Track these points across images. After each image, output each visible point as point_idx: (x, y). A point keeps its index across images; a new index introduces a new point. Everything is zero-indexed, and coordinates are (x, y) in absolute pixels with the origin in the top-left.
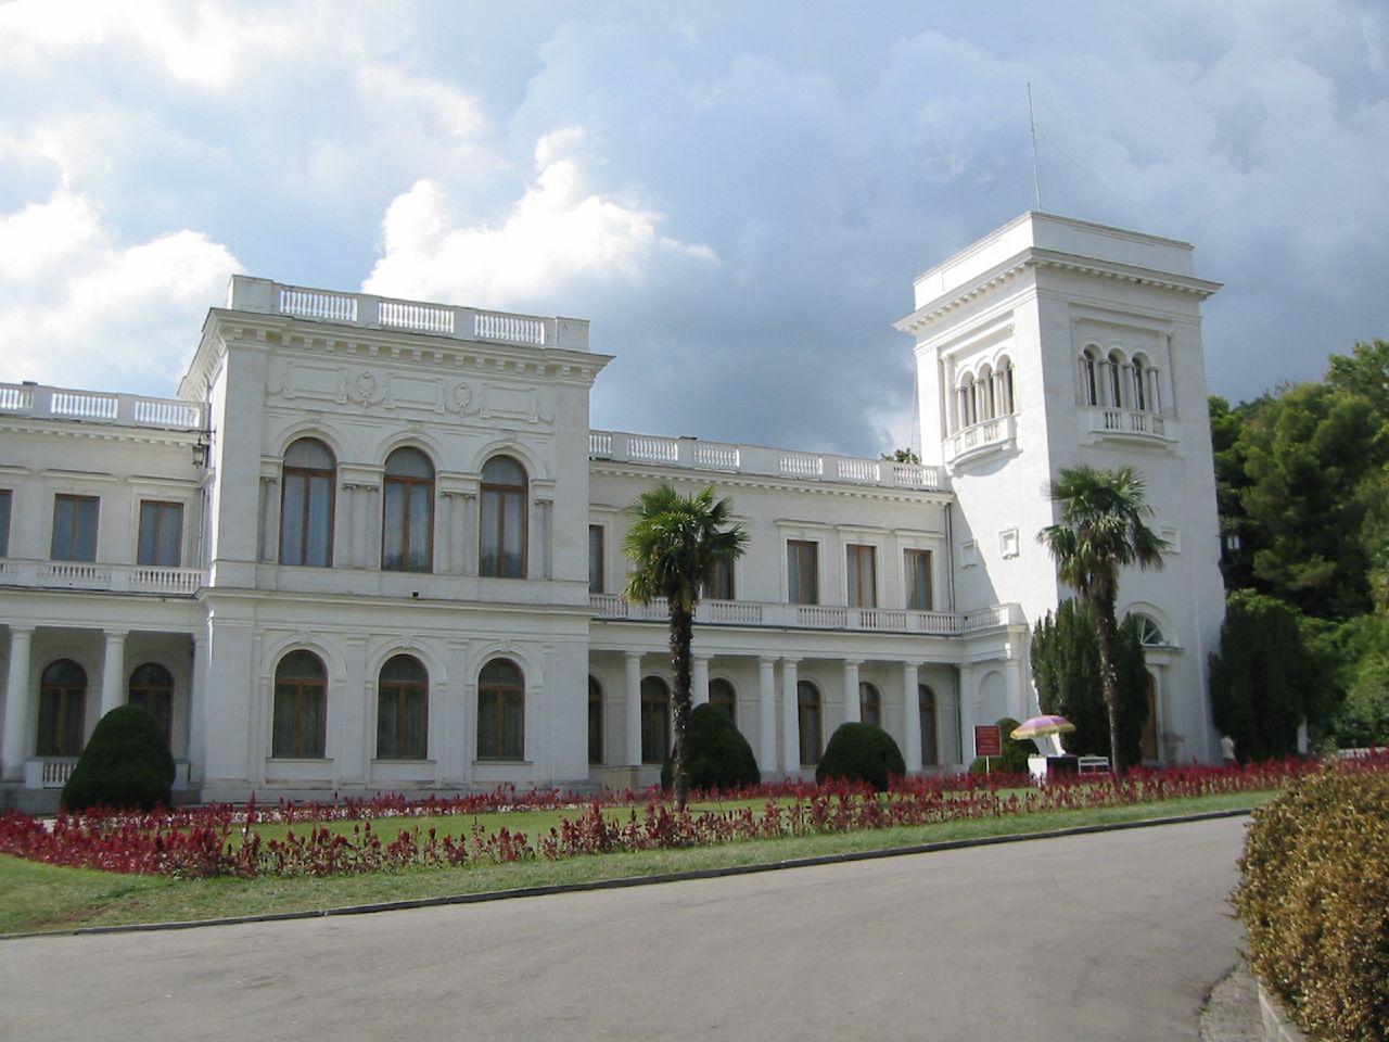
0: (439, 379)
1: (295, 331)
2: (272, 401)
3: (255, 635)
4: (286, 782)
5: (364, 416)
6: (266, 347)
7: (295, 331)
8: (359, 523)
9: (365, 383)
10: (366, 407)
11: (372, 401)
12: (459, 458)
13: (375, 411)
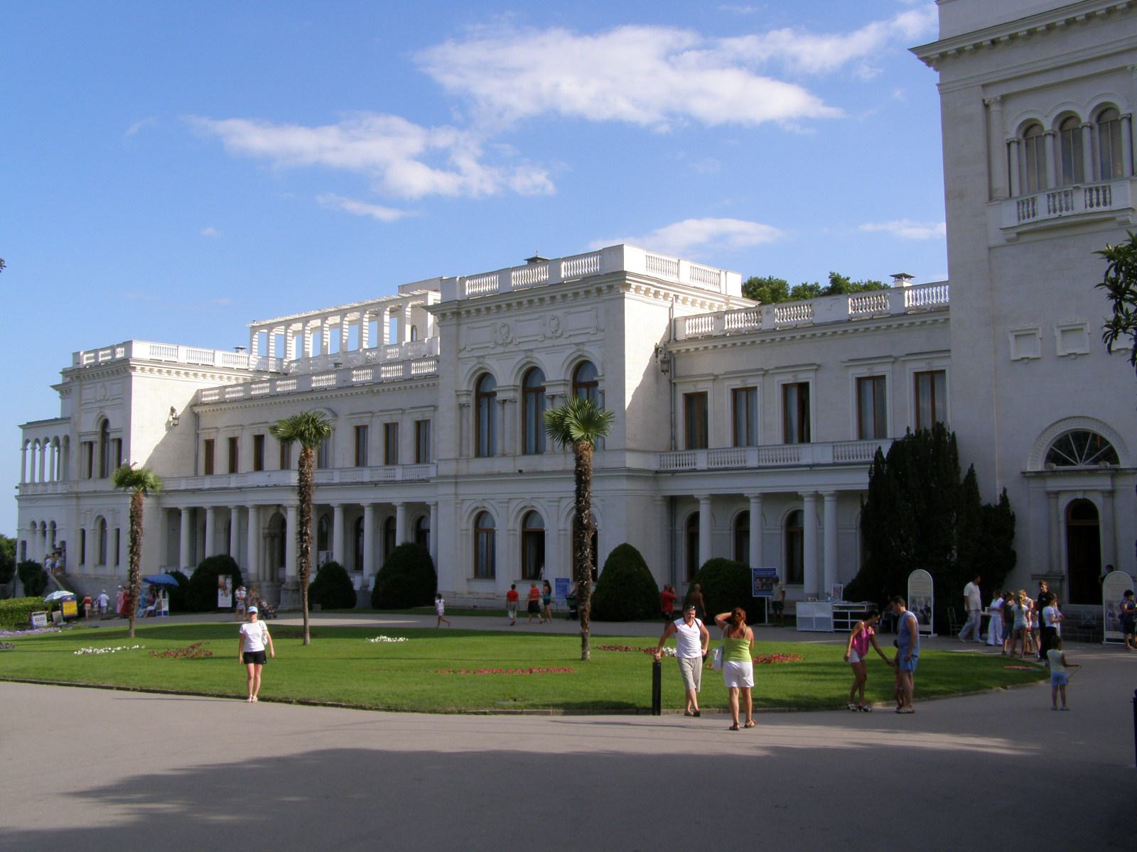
0: (541, 317)
1: (465, 307)
2: (462, 355)
3: (456, 504)
4: (478, 593)
5: (504, 353)
6: (454, 321)
7: (465, 307)
8: (508, 422)
9: (505, 330)
10: (505, 346)
11: (509, 341)
12: (555, 371)
13: (511, 348)
